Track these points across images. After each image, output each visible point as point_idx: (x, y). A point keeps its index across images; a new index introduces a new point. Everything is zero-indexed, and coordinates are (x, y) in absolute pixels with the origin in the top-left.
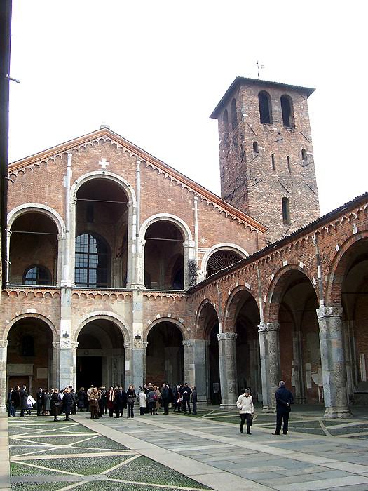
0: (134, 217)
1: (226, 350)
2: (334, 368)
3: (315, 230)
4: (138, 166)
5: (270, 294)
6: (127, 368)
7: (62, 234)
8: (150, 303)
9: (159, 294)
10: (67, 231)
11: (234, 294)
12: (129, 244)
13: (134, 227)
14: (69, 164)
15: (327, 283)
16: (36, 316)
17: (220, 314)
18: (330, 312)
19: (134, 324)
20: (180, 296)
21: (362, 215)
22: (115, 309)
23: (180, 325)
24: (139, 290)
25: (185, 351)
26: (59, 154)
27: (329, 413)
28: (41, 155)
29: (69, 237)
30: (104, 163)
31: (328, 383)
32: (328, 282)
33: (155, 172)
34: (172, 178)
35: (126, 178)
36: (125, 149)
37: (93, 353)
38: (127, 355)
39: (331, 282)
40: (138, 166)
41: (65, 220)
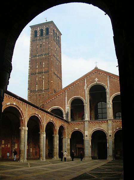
0: (108, 95)
4: (108, 78)
6: (108, 146)
7: (85, 104)
8: (114, 124)
10: (86, 103)
14: (86, 82)
16: (78, 130)
19: (109, 131)
24: (110, 120)
26: (82, 79)
28: (77, 81)
29: (87, 105)
30: (96, 80)
35: (104, 83)
36: (103, 74)
40: (108, 78)
41: (85, 100)
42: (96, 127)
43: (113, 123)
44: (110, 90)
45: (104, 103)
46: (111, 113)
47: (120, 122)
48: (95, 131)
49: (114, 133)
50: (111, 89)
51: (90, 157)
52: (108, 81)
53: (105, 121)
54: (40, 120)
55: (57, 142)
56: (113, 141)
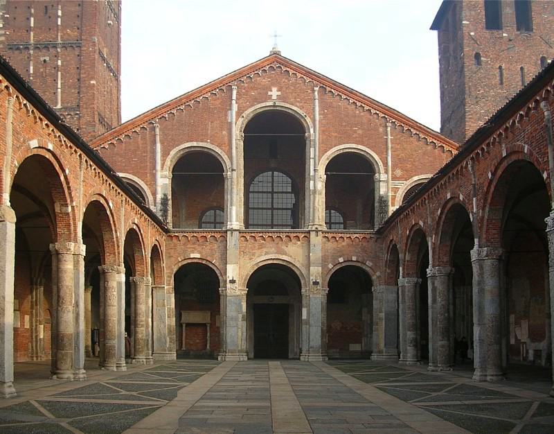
0: (312, 150)
1: (406, 298)
2: (486, 321)
3: (469, 155)
4: (316, 93)
5: (438, 234)
6: (304, 316)
9: (342, 235)
11: (412, 232)
12: (306, 180)
13: (312, 161)
15: (483, 217)
17: (401, 256)
18: (485, 253)
19: (311, 268)
20: (368, 236)
21: (510, 135)
22: (292, 253)
23: (368, 269)
24: (317, 231)
25: (374, 298)
27: (477, 375)
31: (478, 339)
32: (483, 217)
33: (338, 97)
34: (359, 104)
37: (278, 300)
38: (304, 302)
39: (486, 217)
40: (316, 93)
42: (265, 255)
43: (325, 243)
44: (323, 132)
45: (281, 174)
46: (320, 210)
47: (348, 240)
48: (261, 264)
49: (329, 276)
50: (323, 131)
51: (239, 351)
52: (317, 101)
53: (298, 234)
54: (108, 218)
55: (147, 303)
56: (325, 304)
